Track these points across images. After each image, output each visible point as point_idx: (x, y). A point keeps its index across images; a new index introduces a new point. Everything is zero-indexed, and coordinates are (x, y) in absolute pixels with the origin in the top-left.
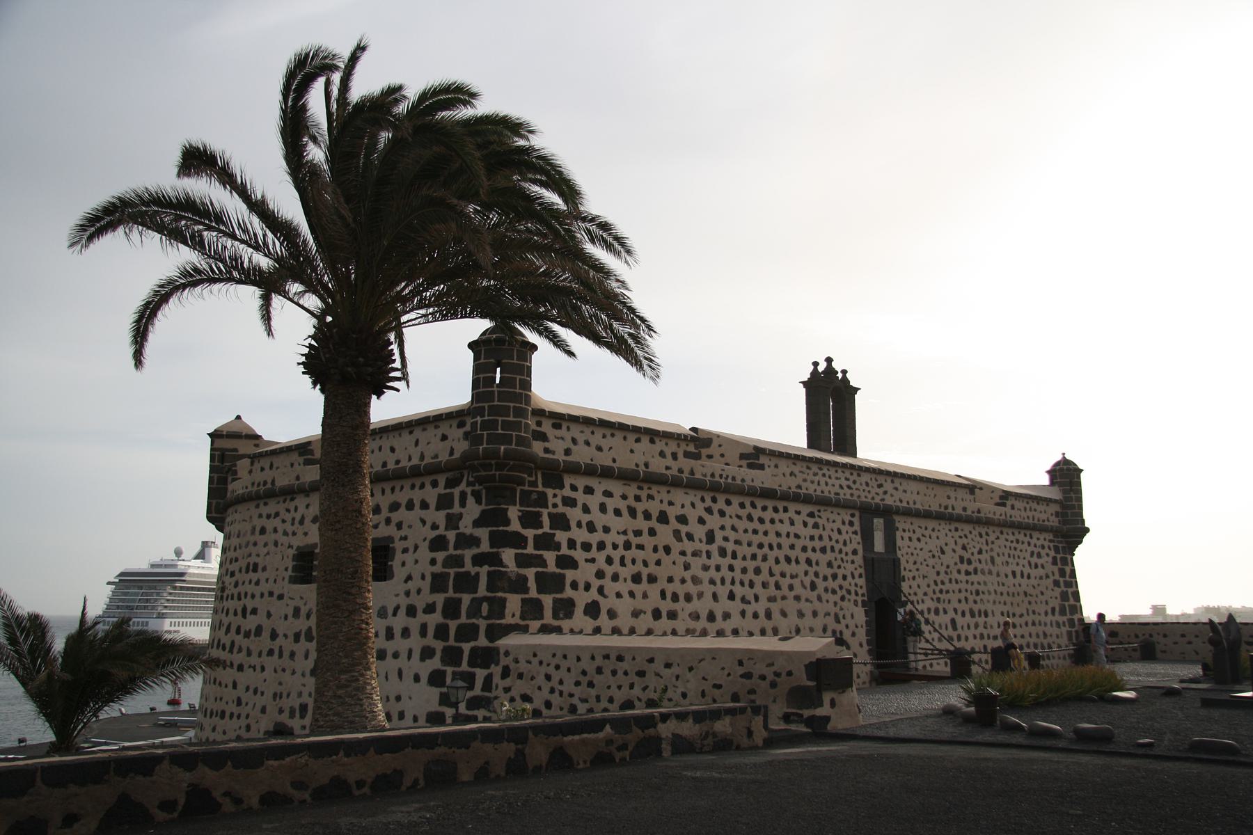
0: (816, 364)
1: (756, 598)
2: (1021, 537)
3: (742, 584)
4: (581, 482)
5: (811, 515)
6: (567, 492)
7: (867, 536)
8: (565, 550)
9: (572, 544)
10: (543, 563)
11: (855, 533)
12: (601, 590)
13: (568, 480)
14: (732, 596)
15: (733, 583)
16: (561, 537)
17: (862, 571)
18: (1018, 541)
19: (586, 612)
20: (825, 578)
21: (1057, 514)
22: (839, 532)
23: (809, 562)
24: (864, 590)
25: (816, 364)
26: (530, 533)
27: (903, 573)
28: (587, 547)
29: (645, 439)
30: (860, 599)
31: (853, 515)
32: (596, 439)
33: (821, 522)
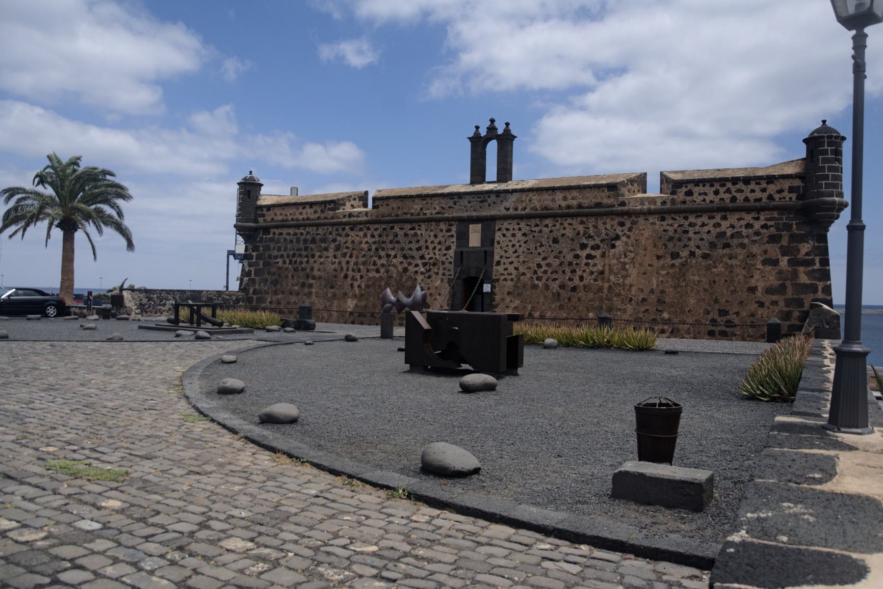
0: (477, 128)
1: (362, 277)
2: (699, 221)
3: (353, 270)
4: (277, 231)
5: (413, 229)
6: (271, 236)
7: (463, 237)
8: (267, 260)
9: (270, 256)
10: (259, 265)
11: (452, 236)
12: (279, 275)
13: (272, 231)
14: (346, 276)
15: (348, 269)
16: (267, 254)
17: (452, 260)
18: (691, 225)
19: (272, 283)
20: (417, 265)
21: (791, 190)
22: (436, 236)
23: (405, 257)
24: (452, 273)
25: (477, 128)
26: (254, 254)
27: (497, 258)
28: (276, 257)
29: (308, 207)
30: (446, 278)
31: (452, 225)
32: (284, 212)
33: (419, 232)
